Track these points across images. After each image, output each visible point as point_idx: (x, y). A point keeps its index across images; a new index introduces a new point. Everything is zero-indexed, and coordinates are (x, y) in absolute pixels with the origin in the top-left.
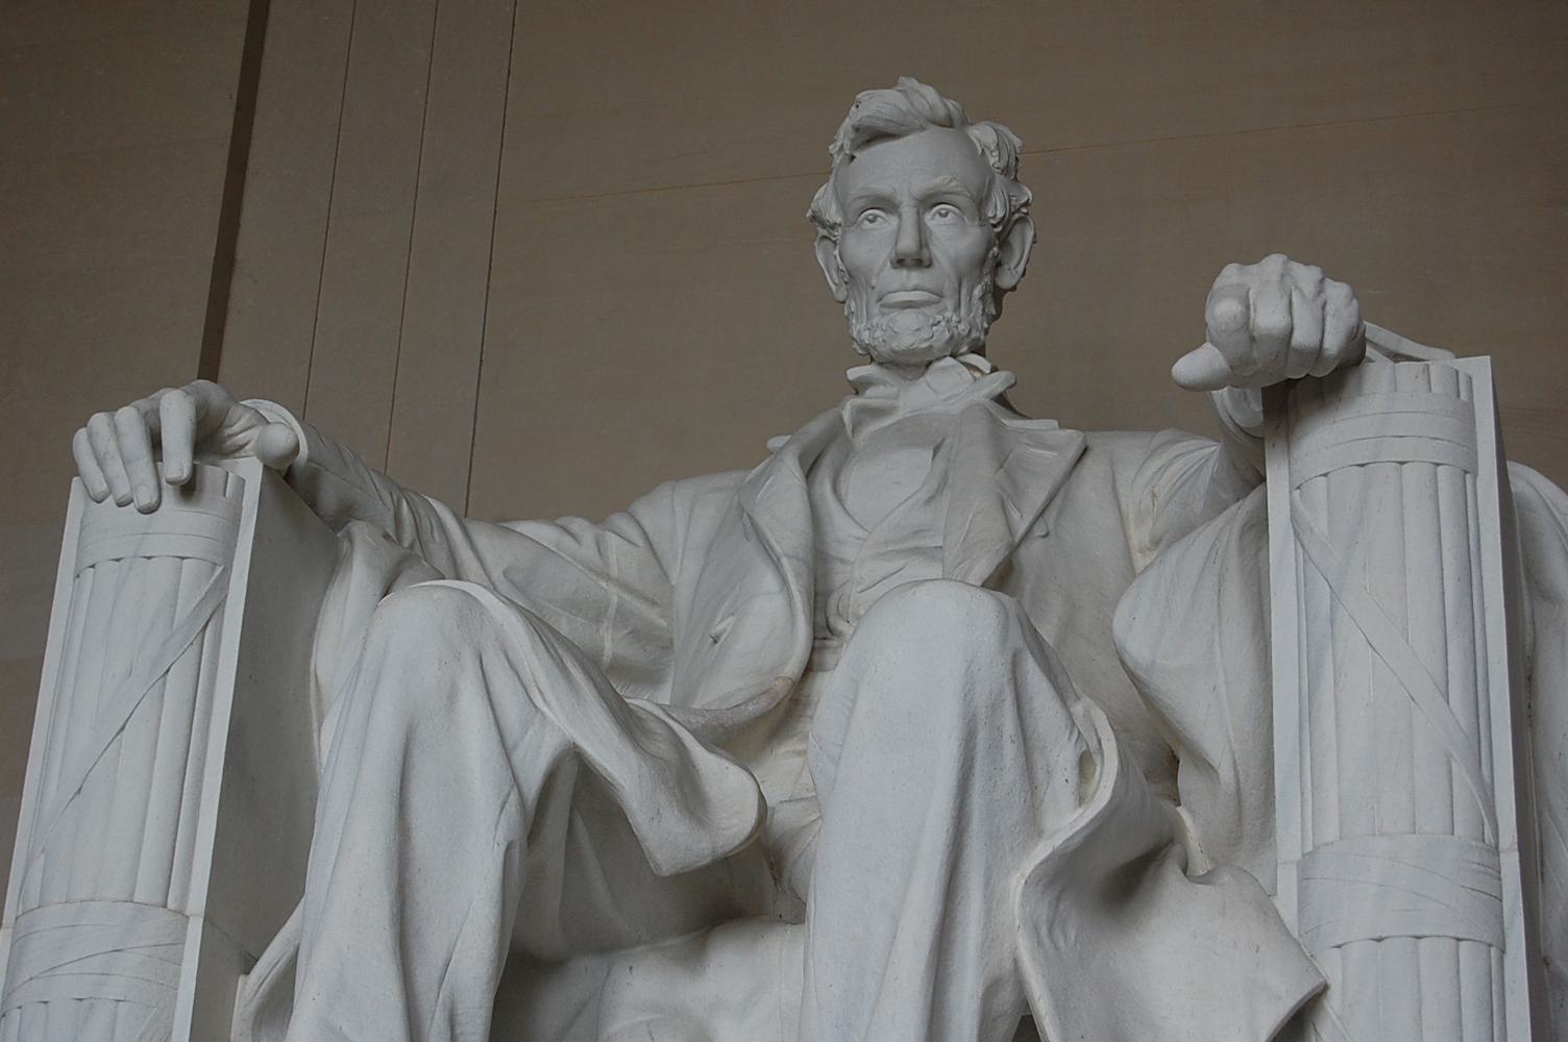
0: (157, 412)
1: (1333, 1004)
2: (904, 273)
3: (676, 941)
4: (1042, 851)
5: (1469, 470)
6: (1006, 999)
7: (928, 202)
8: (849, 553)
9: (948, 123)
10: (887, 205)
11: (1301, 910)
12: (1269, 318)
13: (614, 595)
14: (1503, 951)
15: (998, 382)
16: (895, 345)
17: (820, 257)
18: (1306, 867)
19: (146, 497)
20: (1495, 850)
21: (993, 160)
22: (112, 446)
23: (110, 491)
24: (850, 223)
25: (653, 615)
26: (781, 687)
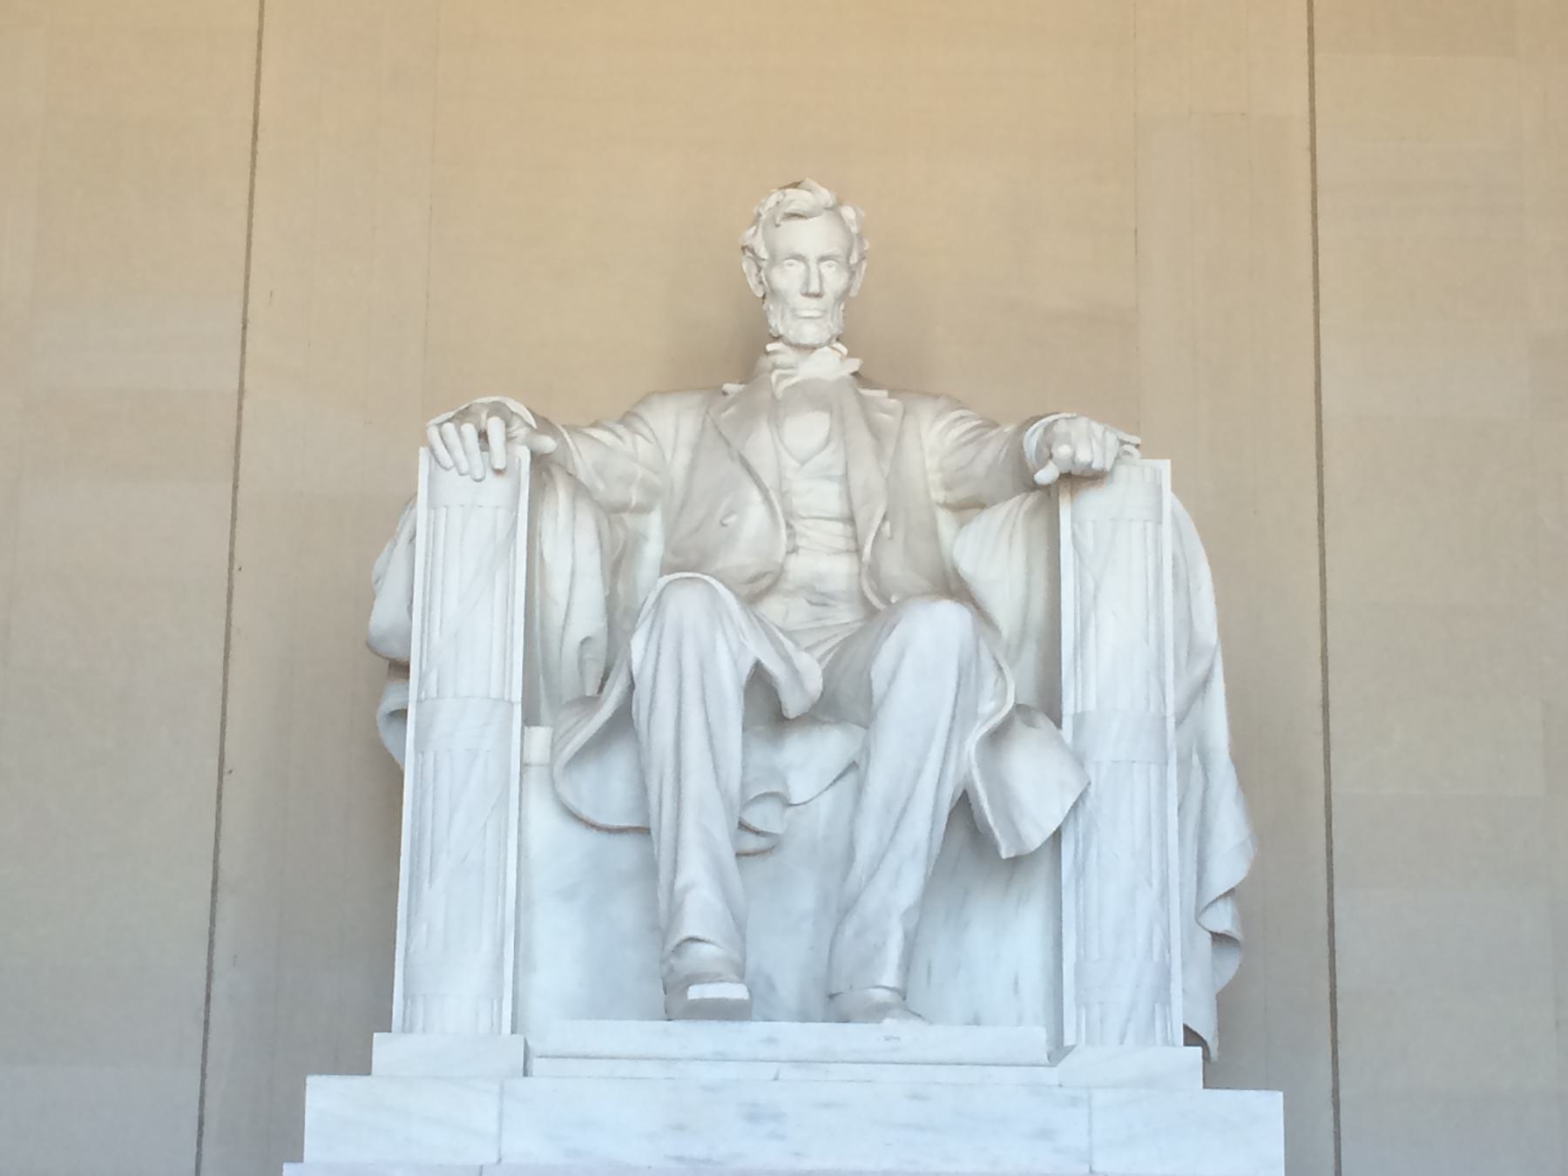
1: (1092, 790)
3: (761, 728)
4: (985, 730)
5: (1159, 522)
7: (822, 259)
10: (800, 258)
12: (1083, 456)
13: (641, 472)
14: (1166, 763)
15: (855, 364)
16: (802, 342)
17: (745, 266)
18: (1079, 719)
20: (1164, 718)
21: (854, 229)
23: (456, 465)
24: (774, 260)
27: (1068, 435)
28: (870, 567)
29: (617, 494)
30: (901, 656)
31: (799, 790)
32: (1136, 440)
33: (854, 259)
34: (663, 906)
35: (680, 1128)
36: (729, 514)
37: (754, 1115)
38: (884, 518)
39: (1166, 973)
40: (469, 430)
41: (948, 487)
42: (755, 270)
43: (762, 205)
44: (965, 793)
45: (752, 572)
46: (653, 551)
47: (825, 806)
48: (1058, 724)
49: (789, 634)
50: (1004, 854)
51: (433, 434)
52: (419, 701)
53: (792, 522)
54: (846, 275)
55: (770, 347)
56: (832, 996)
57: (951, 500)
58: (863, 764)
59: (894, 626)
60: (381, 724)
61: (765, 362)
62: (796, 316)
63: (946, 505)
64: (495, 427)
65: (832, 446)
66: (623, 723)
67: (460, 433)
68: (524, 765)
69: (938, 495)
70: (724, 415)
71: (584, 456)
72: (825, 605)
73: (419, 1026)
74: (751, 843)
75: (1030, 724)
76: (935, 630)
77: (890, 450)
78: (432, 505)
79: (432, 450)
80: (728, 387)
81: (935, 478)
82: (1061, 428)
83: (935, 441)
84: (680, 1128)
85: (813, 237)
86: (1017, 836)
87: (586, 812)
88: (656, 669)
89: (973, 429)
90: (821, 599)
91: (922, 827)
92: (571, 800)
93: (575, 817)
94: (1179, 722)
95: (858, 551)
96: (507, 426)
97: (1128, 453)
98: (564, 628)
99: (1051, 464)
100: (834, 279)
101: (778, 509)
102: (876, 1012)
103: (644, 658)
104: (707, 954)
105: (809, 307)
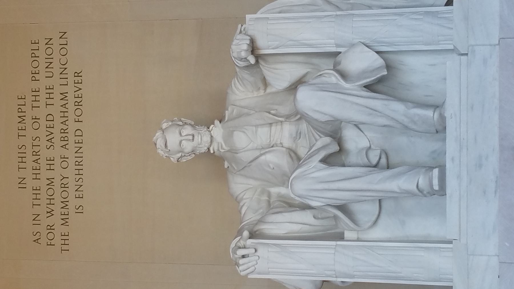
0: (239, 258)
1: (362, 41)
2: (195, 139)
3: (343, 158)
4: (342, 81)
5: (268, 18)
6: (364, 89)
8: (256, 145)
9: (163, 131)
10: (180, 142)
11: (345, 47)
12: (245, 47)
15: (217, 122)
18: (338, 46)
19: (258, 258)
22: (246, 265)
23: (254, 266)
25: (259, 190)
26: (288, 150)
27: (238, 52)
28: (287, 118)
29: (264, 205)
30: (315, 111)
31: (365, 144)
32: (240, 25)
33: (181, 123)
34: (406, 195)
35: (485, 192)
36: (269, 166)
37: (480, 166)
38: (269, 113)
39: (427, 13)
40: (241, 261)
41: (259, 89)
42: (186, 157)
43: (163, 155)
44: (365, 87)
45: (290, 160)
46: (283, 190)
47: (369, 134)
48: (340, 53)
49: (311, 148)
50: (386, 73)
51: (243, 273)
52: (336, 277)
53: (272, 145)
54: (186, 126)
55: (212, 152)
56: (437, 132)
57: (263, 88)
58: (355, 123)
59: (307, 114)
60: (346, 285)
61: (217, 153)
62: (201, 144)
63: (265, 90)
64: (241, 252)
65: (246, 131)
66: (343, 208)
67: (243, 264)
68: (358, 240)
69: (262, 92)
70: (236, 168)
71: (250, 217)
72: (300, 133)
73: (451, 277)
74: (383, 161)
75: (339, 63)
76: (307, 99)
77: (246, 111)
78: (268, 273)
79: (249, 274)
80: (226, 167)
81: (256, 94)
82: (235, 54)
83: (242, 94)
84: (485, 192)
85: (173, 138)
86: (379, 68)
87: (374, 218)
88: (322, 198)
89: (238, 81)
90: (299, 135)
91: (377, 103)
92: (370, 224)
93: (375, 222)
94: (339, 8)
95: (281, 122)
96: (240, 248)
97: (244, 29)
98: (310, 225)
99: (248, 58)
100: (187, 130)
101: (267, 150)
102: (443, 118)
103: (319, 202)
104: (423, 182)
105: (197, 139)
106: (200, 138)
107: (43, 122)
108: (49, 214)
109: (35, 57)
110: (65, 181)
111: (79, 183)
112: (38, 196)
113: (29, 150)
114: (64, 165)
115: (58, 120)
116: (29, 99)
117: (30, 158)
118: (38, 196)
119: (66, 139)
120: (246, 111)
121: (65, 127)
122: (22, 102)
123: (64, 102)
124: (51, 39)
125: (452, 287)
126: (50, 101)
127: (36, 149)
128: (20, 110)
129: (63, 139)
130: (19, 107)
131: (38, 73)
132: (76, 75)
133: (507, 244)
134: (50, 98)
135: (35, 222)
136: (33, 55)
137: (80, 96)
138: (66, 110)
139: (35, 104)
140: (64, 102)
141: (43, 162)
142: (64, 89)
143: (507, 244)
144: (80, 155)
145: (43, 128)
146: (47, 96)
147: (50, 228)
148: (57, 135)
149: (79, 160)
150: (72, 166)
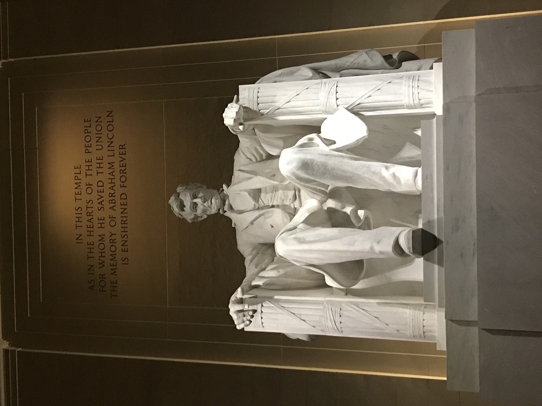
19: (251, 313)
28: (281, 182)
35: (462, 255)
84: (462, 255)
106: (209, 201)
107: (95, 187)
108: (101, 265)
109: (88, 133)
110: (113, 237)
111: (125, 239)
112: (92, 250)
113: (84, 211)
114: (113, 223)
115: (107, 186)
116: (84, 169)
117: (85, 218)
118: (92, 250)
119: (114, 201)
120: (248, 175)
121: (112, 192)
122: (78, 171)
123: (111, 171)
124: (100, 117)
125: (436, 343)
126: (100, 170)
127: (90, 210)
128: (76, 178)
129: (111, 202)
130: (77, 175)
131: (91, 147)
132: (121, 147)
133: (486, 309)
134: (100, 167)
135: (90, 272)
136: (86, 131)
137: (124, 165)
138: (113, 177)
139: (89, 172)
140: (112, 170)
141: (95, 221)
142: (111, 159)
143: (486, 309)
144: (125, 215)
145: (95, 192)
146: (98, 165)
147: (102, 276)
148: (106, 198)
149: (125, 219)
150: (119, 225)
